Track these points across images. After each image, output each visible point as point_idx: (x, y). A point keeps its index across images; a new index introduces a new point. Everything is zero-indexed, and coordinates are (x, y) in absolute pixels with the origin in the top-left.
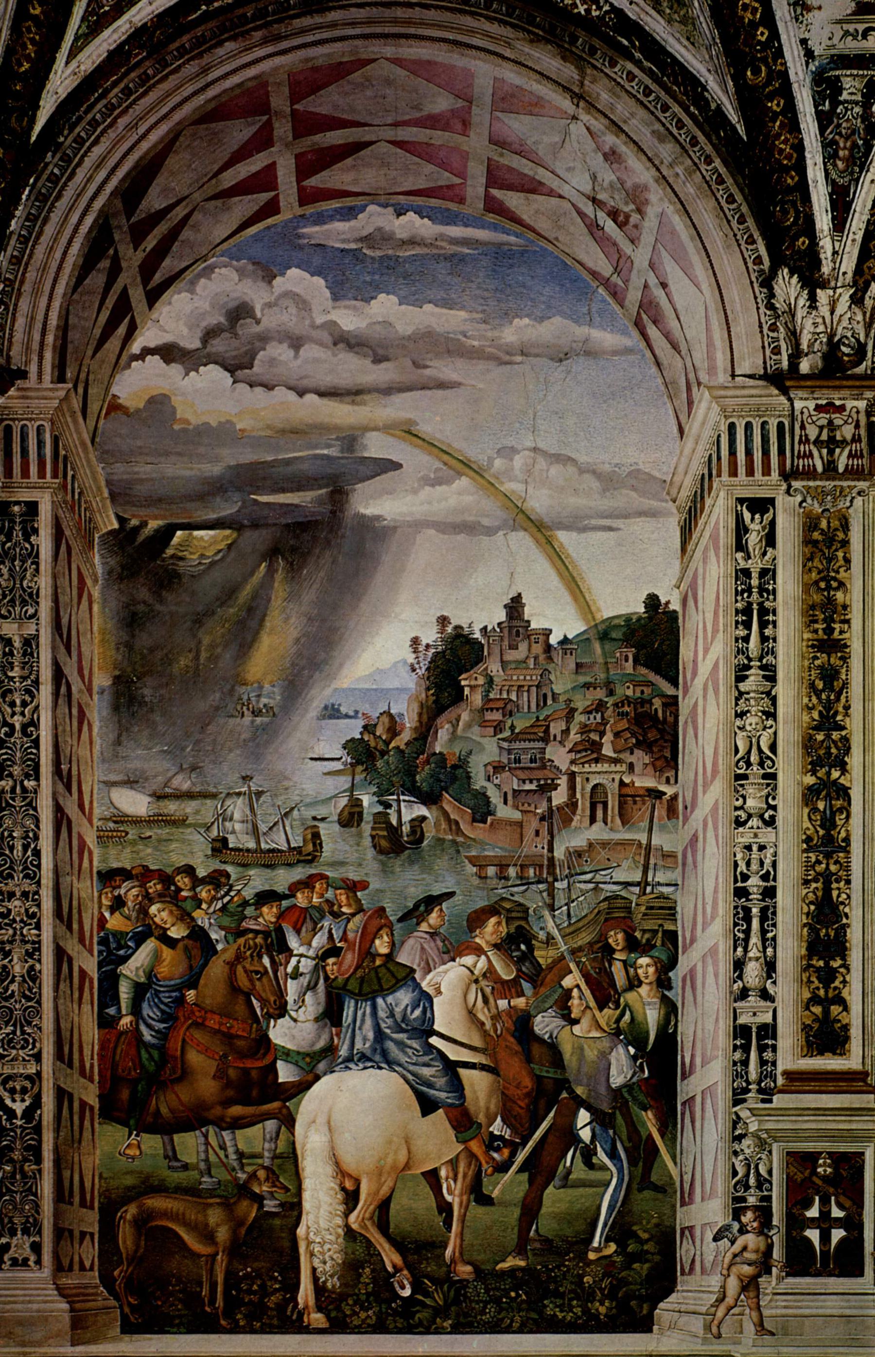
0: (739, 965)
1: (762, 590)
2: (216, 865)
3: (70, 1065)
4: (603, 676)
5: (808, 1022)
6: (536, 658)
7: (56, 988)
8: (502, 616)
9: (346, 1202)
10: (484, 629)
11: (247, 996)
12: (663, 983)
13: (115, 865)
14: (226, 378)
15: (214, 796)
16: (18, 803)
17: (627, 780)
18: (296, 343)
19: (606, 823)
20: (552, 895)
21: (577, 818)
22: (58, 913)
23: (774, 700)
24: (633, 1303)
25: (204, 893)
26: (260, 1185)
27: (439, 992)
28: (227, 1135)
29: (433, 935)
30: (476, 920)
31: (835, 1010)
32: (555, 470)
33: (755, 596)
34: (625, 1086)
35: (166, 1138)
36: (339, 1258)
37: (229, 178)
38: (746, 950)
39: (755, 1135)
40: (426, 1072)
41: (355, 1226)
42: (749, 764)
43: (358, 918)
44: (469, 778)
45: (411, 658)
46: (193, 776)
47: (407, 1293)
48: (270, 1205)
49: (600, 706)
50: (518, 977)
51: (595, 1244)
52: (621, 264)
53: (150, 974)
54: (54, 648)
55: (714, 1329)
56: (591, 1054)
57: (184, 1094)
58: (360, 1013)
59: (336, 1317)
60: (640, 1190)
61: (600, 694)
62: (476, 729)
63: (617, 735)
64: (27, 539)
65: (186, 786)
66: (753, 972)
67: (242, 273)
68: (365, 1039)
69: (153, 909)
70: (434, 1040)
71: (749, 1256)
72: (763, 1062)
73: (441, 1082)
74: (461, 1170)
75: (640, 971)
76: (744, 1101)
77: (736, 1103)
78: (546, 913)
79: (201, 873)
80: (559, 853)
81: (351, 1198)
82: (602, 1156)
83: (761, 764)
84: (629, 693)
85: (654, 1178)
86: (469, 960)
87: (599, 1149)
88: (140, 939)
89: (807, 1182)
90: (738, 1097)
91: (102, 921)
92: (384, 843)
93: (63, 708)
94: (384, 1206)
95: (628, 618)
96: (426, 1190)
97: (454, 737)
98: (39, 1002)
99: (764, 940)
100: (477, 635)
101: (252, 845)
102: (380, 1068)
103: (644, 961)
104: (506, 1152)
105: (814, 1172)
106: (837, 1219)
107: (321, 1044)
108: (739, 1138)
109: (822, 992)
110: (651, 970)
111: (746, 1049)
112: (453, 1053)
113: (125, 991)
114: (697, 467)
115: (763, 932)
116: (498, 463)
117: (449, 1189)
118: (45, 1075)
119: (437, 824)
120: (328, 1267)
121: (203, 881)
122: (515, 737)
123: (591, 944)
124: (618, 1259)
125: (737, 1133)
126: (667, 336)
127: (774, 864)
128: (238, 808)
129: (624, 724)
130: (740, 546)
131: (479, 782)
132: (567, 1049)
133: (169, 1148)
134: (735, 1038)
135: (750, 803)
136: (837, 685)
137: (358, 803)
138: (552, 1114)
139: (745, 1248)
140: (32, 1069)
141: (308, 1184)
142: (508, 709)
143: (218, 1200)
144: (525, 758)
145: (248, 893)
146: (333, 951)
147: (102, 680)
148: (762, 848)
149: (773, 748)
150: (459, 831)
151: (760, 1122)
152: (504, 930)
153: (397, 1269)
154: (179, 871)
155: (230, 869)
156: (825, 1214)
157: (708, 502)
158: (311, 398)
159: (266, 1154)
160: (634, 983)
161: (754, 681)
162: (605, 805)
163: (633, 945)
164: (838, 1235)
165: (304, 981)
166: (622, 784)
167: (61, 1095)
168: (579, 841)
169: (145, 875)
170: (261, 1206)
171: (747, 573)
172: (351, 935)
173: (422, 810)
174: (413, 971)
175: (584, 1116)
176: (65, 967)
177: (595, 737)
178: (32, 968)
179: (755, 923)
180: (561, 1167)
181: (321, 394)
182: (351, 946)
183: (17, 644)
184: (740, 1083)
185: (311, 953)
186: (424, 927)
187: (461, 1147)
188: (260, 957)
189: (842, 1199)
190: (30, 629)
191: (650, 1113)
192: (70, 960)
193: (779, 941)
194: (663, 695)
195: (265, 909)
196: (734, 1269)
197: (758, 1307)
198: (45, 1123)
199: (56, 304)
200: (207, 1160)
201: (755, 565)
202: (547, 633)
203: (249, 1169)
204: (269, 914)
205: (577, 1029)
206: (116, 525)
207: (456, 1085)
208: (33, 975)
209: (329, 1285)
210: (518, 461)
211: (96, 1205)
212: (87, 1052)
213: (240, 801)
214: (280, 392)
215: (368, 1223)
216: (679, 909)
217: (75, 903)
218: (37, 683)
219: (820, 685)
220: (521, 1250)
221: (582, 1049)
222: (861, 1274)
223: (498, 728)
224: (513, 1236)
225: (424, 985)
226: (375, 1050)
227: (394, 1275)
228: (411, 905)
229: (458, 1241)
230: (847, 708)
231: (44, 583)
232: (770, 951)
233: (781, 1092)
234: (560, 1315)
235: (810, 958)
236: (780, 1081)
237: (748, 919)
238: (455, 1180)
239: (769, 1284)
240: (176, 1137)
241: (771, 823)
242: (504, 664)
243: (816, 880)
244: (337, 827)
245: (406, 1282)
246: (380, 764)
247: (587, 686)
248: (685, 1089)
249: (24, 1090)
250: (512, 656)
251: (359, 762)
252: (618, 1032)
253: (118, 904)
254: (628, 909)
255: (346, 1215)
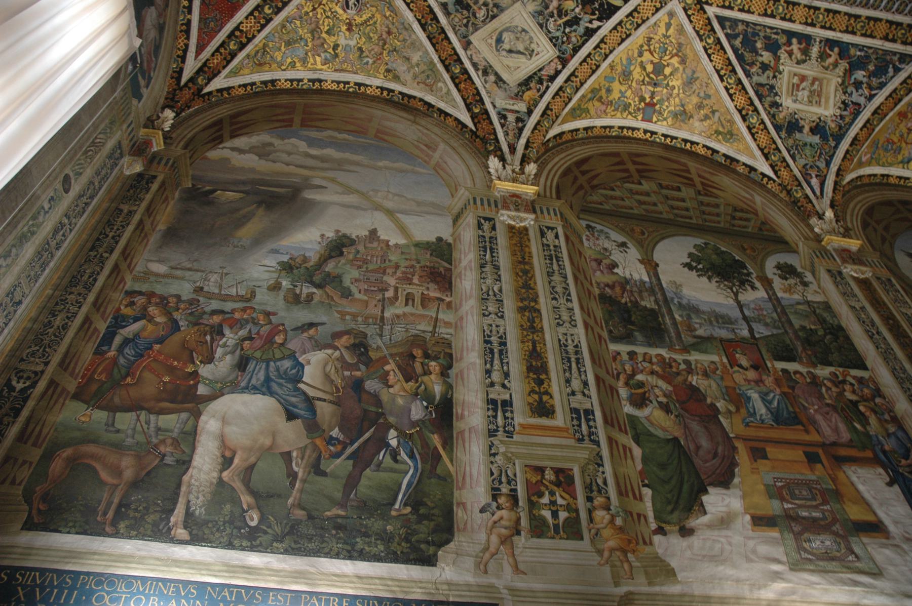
0: (488, 372)
1: (490, 242)
2: (194, 296)
3: (65, 370)
4: (414, 257)
5: (531, 401)
6: (382, 248)
7: (77, 334)
8: (367, 233)
9: (223, 464)
10: (357, 236)
11: (192, 352)
12: (444, 373)
13: (137, 289)
14: (257, 158)
15: (203, 271)
16: (96, 260)
17: (426, 292)
18: (289, 154)
19: (413, 306)
20: (381, 329)
21: (397, 304)
22: (95, 304)
23: (499, 276)
24: (423, 546)
25: (182, 306)
26: (166, 447)
27: (309, 363)
28: (153, 418)
29: (310, 338)
30: (337, 335)
31: (545, 398)
32: (396, 198)
33: (488, 244)
34: (420, 420)
35: (111, 414)
36: (209, 497)
37: (275, 118)
38: (492, 365)
39: (504, 454)
40: (293, 399)
41: (225, 479)
42: (488, 295)
43: (268, 326)
44: (341, 281)
45: (319, 240)
46: (195, 263)
47: (253, 524)
48: (169, 460)
49: (412, 267)
50: (358, 362)
51: (397, 506)
52: (430, 157)
53: (137, 335)
54: (143, 215)
55: (482, 567)
56: (400, 401)
57: (133, 392)
58: (258, 367)
59: (197, 535)
60: (430, 478)
61: (414, 263)
62: (348, 266)
63: (421, 277)
64: (147, 183)
65: (189, 266)
66: (496, 376)
67: (272, 137)
68: (258, 380)
69: (150, 309)
70: (301, 386)
71: (503, 523)
72: (506, 418)
73: (301, 405)
74: (307, 454)
75: (431, 368)
76: (496, 436)
77: (490, 436)
78: (378, 338)
79: (184, 298)
80: (387, 314)
81: (227, 462)
82: (403, 456)
83: (495, 295)
84: (428, 264)
85: (439, 471)
86: (330, 351)
87: (402, 452)
88: (136, 319)
89: (540, 482)
90: (492, 433)
91: (119, 309)
92: (290, 299)
93: (138, 232)
94: (251, 467)
95: (428, 243)
96: (281, 463)
97: (336, 266)
98: (62, 339)
99: (502, 363)
100: (354, 237)
101: (217, 291)
102: (264, 394)
103: (433, 363)
104: (339, 447)
105: (543, 477)
106: (561, 506)
107: (231, 378)
108: (494, 455)
109: (537, 389)
110: (437, 368)
111: (495, 410)
112: (311, 393)
113: (117, 340)
114: (460, 205)
115: (501, 360)
116: (371, 193)
117: (297, 464)
118: (46, 372)
119: (321, 296)
120: (199, 501)
121: (184, 301)
122: (367, 271)
123: (402, 353)
124: (413, 518)
125: (493, 451)
126: (447, 173)
127: (505, 333)
128: (214, 278)
129: (425, 273)
130: (479, 228)
131: (347, 282)
132: (385, 397)
133: (111, 419)
134: (488, 404)
135: (490, 309)
136: (529, 275)
137: (281, 284)
138: (372, 430)
139: (501, 518)
140: (39, 368)
141: (199, 450)
142: (365, 262)
143: (132, 453)
144: (373, 279)
145: (208, 309)
146: (250, 338)
147: (162, 227)
148: (497, 326)
149: (500, 290)
150: (332, 299)
151: (506, 448)
152: (352, 341)
153: (250, 507)
154: (172, 296)
155: (201, 299)
156: (553, 503)
157: (465, 215)
158: (291, 167)
159: (176, 430)
160: (427, 373)
161: (488, 268)
162: (413, 300)
163: (427, 356)
164: (563, 515)
165: (229, 349)
166: (422, 293)
167: (52, 383)
168: (399, 311)
169: (151, 295)
170: (162, 459)
171: (484, 237)
172: (261, 333)
173: (315, 290)
174: (295, 352)
175: (392, 433)
176: (86, 326)
177: (410, 276)
178: (66, 324)
179: (496, 356)
180: (376, 459)
181: (297, 166)
182: (261, 337)
183: (125, 211)
184: (492, 427)
185: (236, 337)
186: (305, 334)
187: (309, 441)
188: (205, 335)
189: (564, 494)
190: (135, 208)
191: (436, 436)
192: (91, 323)
193: (511, 363)
194: (444, 267)
195: (215, 317)
196: (494, 530)
197: (513, 555)
198: (32, 396)
199: (192, 133)
200: (134, 429)
201: (487, 235)
202: (388, 241)
203: (161, 437)
204: (216, 319)
205: (391, 390)
206: (190, 186)
207: (312, 409)
208: (65, 327)
209: (197, 513)
210: (379, 194)
211: (44, 445)
212: (80, 364)
213: (216, 276)
214: (278, 164)
215: (236, 478)
216: (453, 344)
217: (107, 300)
218: (128, 224)
219: (520, 274)
220: (342, 505)
221: (394, 400)
222: (582, 539)
223: (359, 267)
224: (338, 495)
225: (300, 360)
226: (263, 386)
227: (247, 512)
228: (300, 325)
229: (298, 495)
230: (535, 283)
231: (149, 197)
232: (505, 368)
233: (518, 433)
234: (366, 548)
235: (528, 373)
236: (517, 428)
237: (492, 352)
238: (302, 459)
239: (521, 541)
240: (118, 415)
241: (502, 317)
242: (366, 248)
243: (528, 341)
244: (266, 291)
245: (255, 516)
246: (295, 271)
247: (407, 259)
248: (458, 425)
249: (29, 378)
250: (371, 245)
251: (284, 269)
252: (417, 394)
253: (132, 304)
254: (425, 342)
255: (221, 471)
